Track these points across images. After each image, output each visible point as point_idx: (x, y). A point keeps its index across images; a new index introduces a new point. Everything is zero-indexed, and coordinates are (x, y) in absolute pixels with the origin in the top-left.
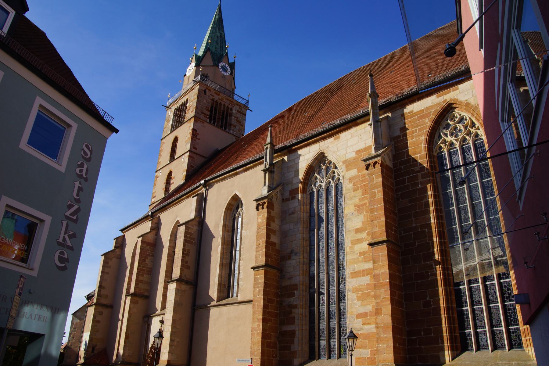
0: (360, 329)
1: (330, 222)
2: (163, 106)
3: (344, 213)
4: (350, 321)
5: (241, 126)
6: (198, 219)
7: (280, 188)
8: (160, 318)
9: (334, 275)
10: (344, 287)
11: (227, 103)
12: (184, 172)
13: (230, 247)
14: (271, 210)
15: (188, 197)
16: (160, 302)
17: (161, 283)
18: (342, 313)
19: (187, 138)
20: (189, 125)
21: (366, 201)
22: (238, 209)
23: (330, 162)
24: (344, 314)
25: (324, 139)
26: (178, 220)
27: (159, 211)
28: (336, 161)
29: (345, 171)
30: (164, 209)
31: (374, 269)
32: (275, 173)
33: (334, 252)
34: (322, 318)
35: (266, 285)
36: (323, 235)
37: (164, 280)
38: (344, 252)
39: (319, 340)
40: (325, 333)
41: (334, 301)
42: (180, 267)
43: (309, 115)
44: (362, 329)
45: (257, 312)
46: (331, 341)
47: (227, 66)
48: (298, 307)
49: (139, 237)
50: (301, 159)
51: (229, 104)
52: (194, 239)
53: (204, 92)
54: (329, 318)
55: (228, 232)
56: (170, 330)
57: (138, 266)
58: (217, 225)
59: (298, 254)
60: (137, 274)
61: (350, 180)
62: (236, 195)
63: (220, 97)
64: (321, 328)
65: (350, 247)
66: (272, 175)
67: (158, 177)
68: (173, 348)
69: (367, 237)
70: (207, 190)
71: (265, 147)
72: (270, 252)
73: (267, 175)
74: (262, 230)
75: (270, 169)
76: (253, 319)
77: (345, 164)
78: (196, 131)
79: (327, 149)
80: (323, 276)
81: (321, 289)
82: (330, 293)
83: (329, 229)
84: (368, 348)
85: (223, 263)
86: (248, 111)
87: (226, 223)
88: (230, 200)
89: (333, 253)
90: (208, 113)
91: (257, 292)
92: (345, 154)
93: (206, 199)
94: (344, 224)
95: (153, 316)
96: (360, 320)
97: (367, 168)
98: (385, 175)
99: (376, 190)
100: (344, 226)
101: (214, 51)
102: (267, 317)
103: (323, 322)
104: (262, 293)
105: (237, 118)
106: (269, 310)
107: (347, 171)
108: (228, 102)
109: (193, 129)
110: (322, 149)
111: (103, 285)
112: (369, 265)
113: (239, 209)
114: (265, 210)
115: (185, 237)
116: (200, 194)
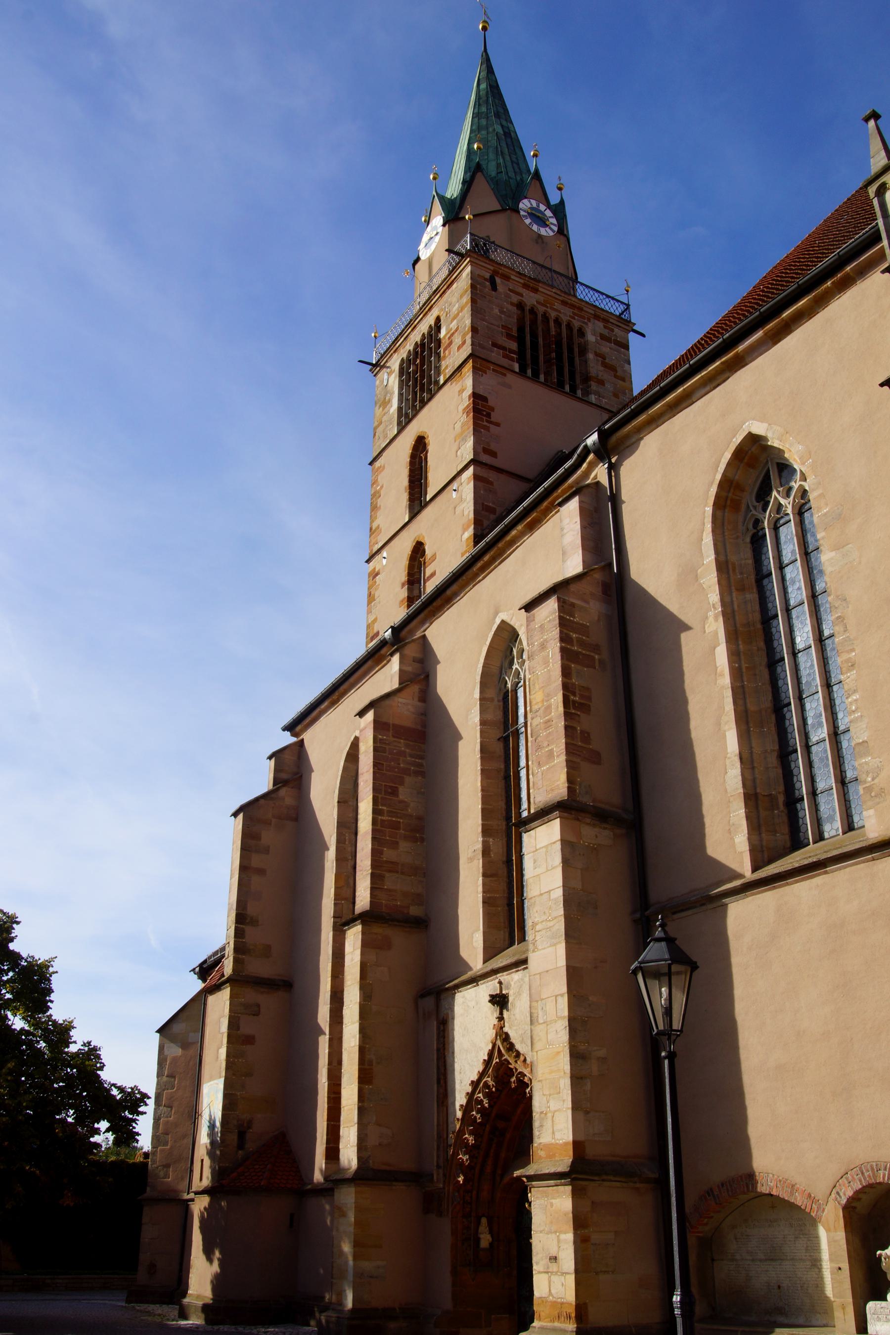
2: (360, 361)
5: (621, 382)
6: (598, 576)
8: (488, 987)
11: (566, 314)
12: (465, 530)
13: (762, 644)
16: (478, 930)
17: (471, 860)
19: (458, 426)
20: (459, 389)
22: (771, 491)
37: (479, 846)
42: (563, 758)
47: (542, 207)
49: (361, 714)
51: (570, 316)
52: (596, 648)
53: (488, 284)
55: (742, 589)
56: (566, 1013)
57: (376, 811)
62: (754, 442)
63: (541, 298)
67: (377, 574)
68: (588, 1086)
70: (613, 469)
78: (485, 399)
85: (746, 711)
86: (632, 336)
87: (726, 556)
88: (729, 464)
90: (514, 346)
93: (615, 499)
95: (457, 987)
101: (493, 174)
105: (603, 357)
109: (475, 396)
111: (251, 910)
113: (774, 493)
115: (562, 640)
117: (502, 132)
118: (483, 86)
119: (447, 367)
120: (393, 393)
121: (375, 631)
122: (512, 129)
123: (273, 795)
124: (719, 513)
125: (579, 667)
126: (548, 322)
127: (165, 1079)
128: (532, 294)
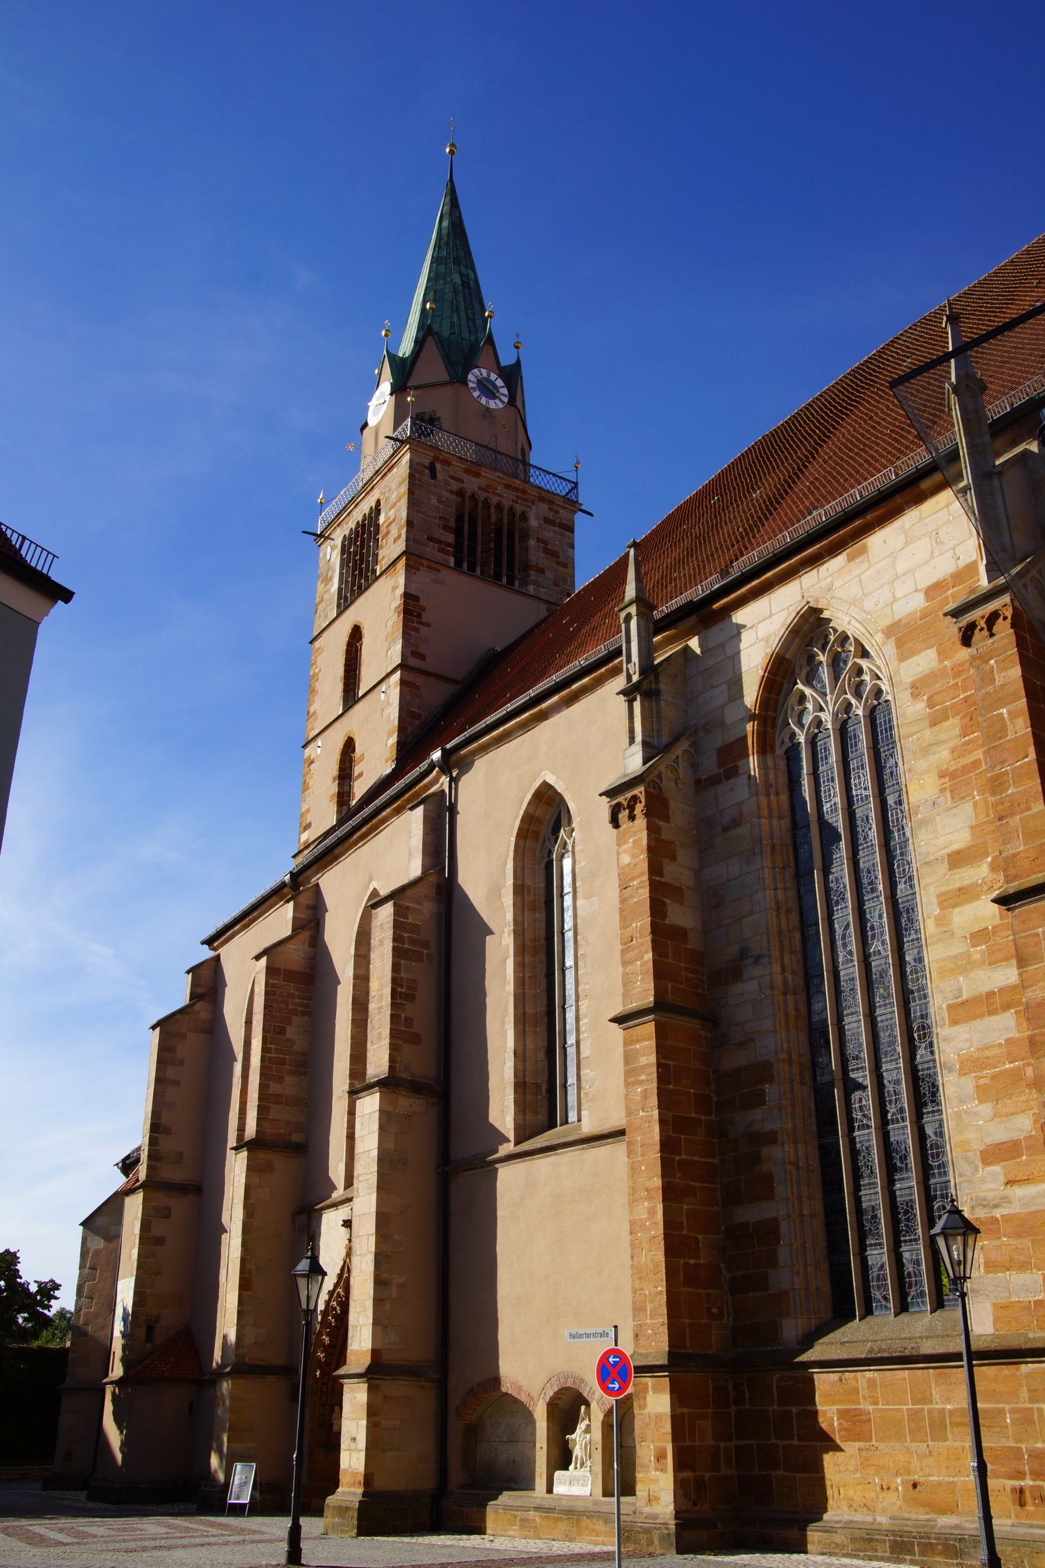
0: (999, 1201)
1: (861, 841)
2: (304, 532)
3: (905, 805)
4: (960, 1175)
6: (433, 879)
7: (684, 745)
9: (891, 1019)
10: (930, 1058)
12: (390, 736)
13: (544, 958)
14: (660, 820)
15: (398, 811)
16: (342, 1161)
17: (340, 1098)
18: (932, 1149)
19: (390, 624)
20: (392, 585)
21: (979, 754)
23: (844, 638)
24: (938, 1154)
25: (815, 561)
26: (375, 889)
27: (315, 867)
28: (863, 630)
29: (896, 662)
30: (328, 858)
31: (1023, 984)
32: (664, 696)
33: (883, 942)
34: (866, 1172)
35: (664, 1074)
36: (842, 886)
38: (918, 939)
39: (862, 1248)
40: (880, 1223)
41: (901, 1110)
42: (387, 1041)
43: (767, 495)
44: (1006, 1200)
45: (643, 1168)
46: (904, 1248)
48: (780, 1141)
49: (257, 958)
50: (746, 638)
52: (425, 944)
53: (427, 471)
54: (891, 1170)
55: (533, 909)
56: (374, 1250)
57: (264, 1050)
58: (495, 891)
59: (765, 960)
60: (262, 1074)
61: (916, 689)
63: (483, 482)
64: (864, 1205)
65: (937, 918)
66: (654, 703)
69: (992, 876)
70: (454, 781)
71: (623, 615)
72: (670, 961)
73: (637, 705)
74: (637, 889)
75: (645, 686)
76: (633, 1190)
77: (894, 638)
78: (416, 598)
79: (828, 596)
80: (855, 1025)
81: (853, 1070)
82: (886, 1082)
83: (862, 865)
84: (1036, 1267)
85: (524, 1014)
86: (579, 517)
87: (523, 880)
88: (529, 804)
89: (882, 946)
90: (450, 538)
91: (638, 1098)
92: (891, 604)
93: (453, 809)
94: (911, 841)
95: (324, 1208)
96: (997, 1168)
97: (967, 639)
98: (1032, 656)
99: (1005, 711)
100: (911, 847)
101: (446, 334)
102: (678, 1180)
103: (869, 1184)
104: (654, 1100)
106: (684, 1157)
107: (902, 658)
108: (511, 495)
109: (407, 596)
110: (811, 596)
111: (165, 1119)
112: (1007, 975)
113: (562, 831)
114: (641, 822)
115: (394, 940)
116: (433, 794)
117: (460, 282)
118: (445, 224)
119: (383, 558)
120: (335, 570)
121: (308, 822)
122: (472, 276)
123: (189, 1010)
124: (521, 843)
125: (408, 962)
126: (489, 507)
127: (87, 1270)
128: (474, 479)
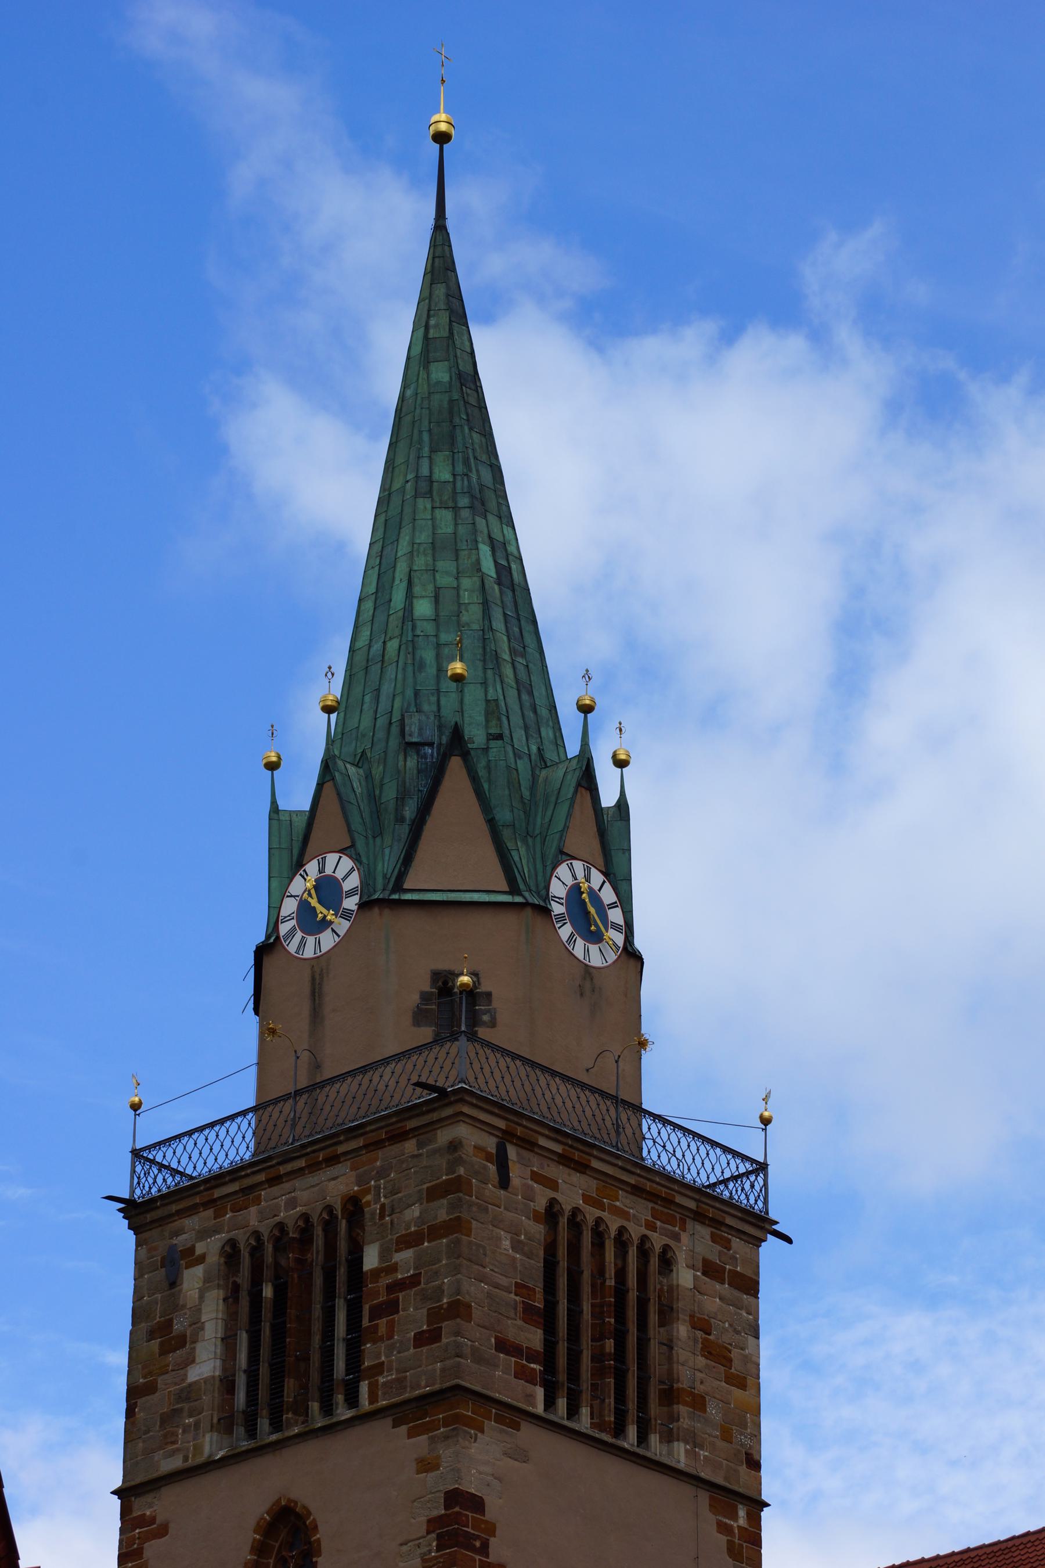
5: (737, 1392)
53: (492, 1168)
120: (197, 1325)
